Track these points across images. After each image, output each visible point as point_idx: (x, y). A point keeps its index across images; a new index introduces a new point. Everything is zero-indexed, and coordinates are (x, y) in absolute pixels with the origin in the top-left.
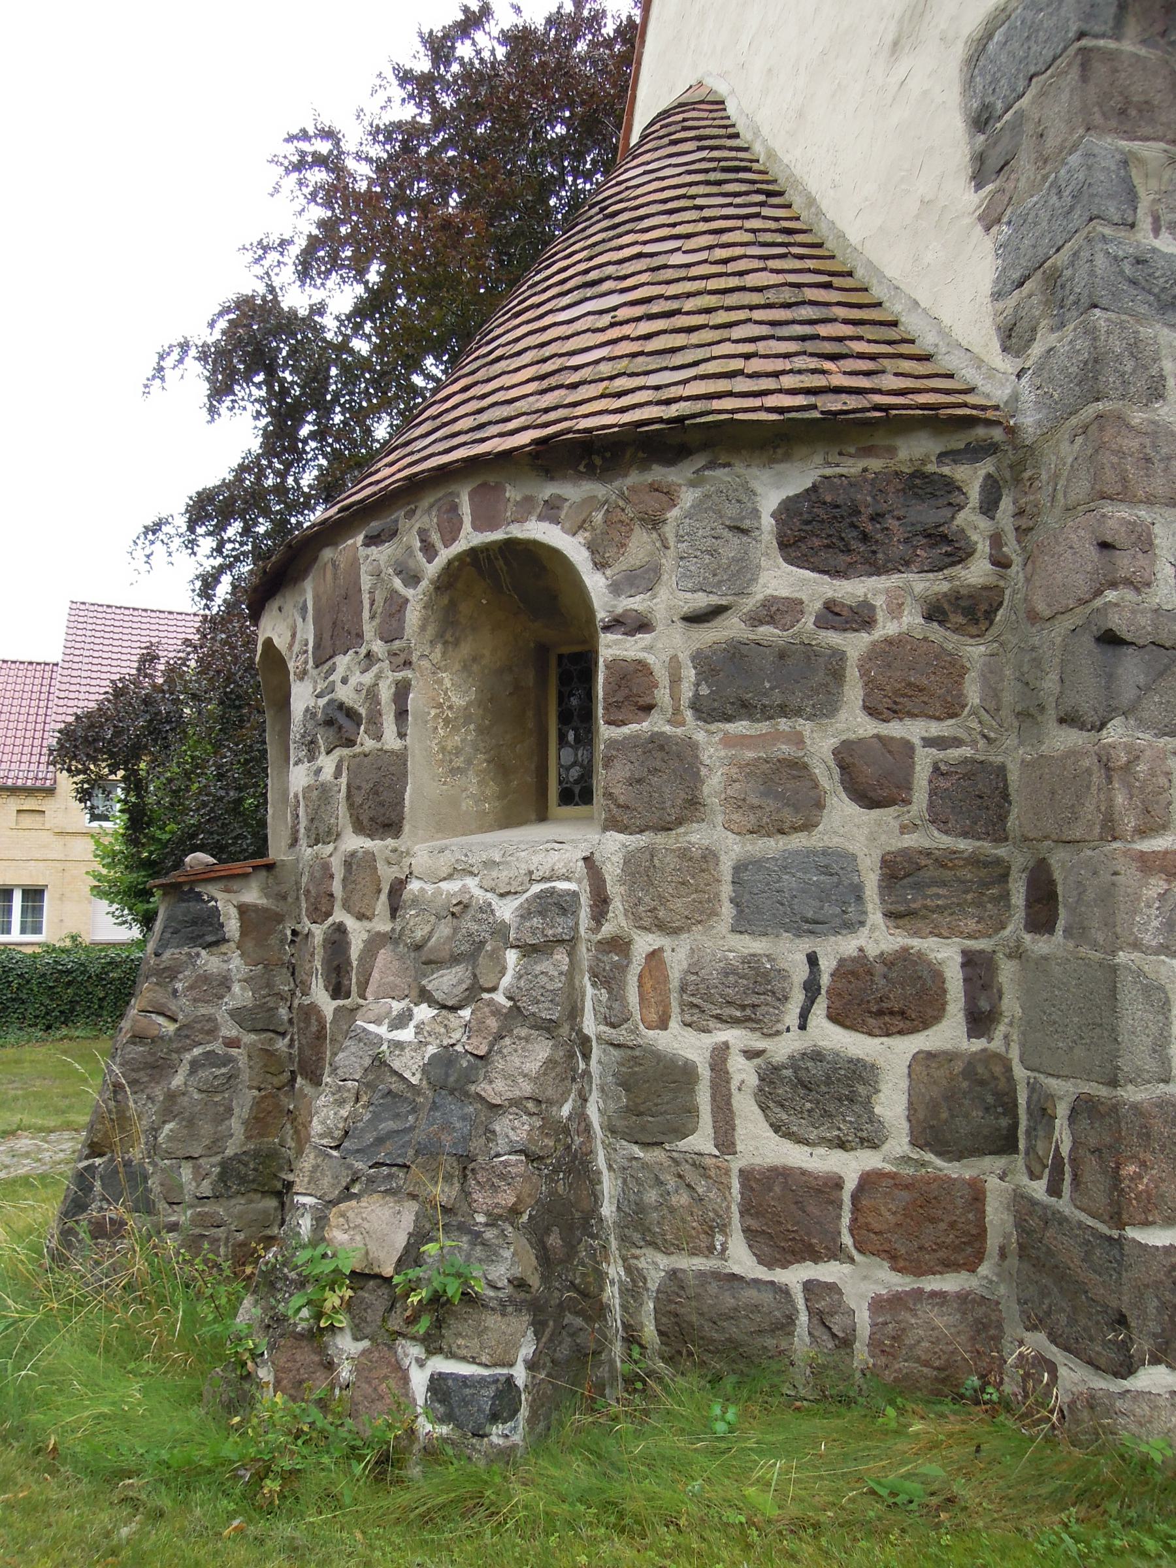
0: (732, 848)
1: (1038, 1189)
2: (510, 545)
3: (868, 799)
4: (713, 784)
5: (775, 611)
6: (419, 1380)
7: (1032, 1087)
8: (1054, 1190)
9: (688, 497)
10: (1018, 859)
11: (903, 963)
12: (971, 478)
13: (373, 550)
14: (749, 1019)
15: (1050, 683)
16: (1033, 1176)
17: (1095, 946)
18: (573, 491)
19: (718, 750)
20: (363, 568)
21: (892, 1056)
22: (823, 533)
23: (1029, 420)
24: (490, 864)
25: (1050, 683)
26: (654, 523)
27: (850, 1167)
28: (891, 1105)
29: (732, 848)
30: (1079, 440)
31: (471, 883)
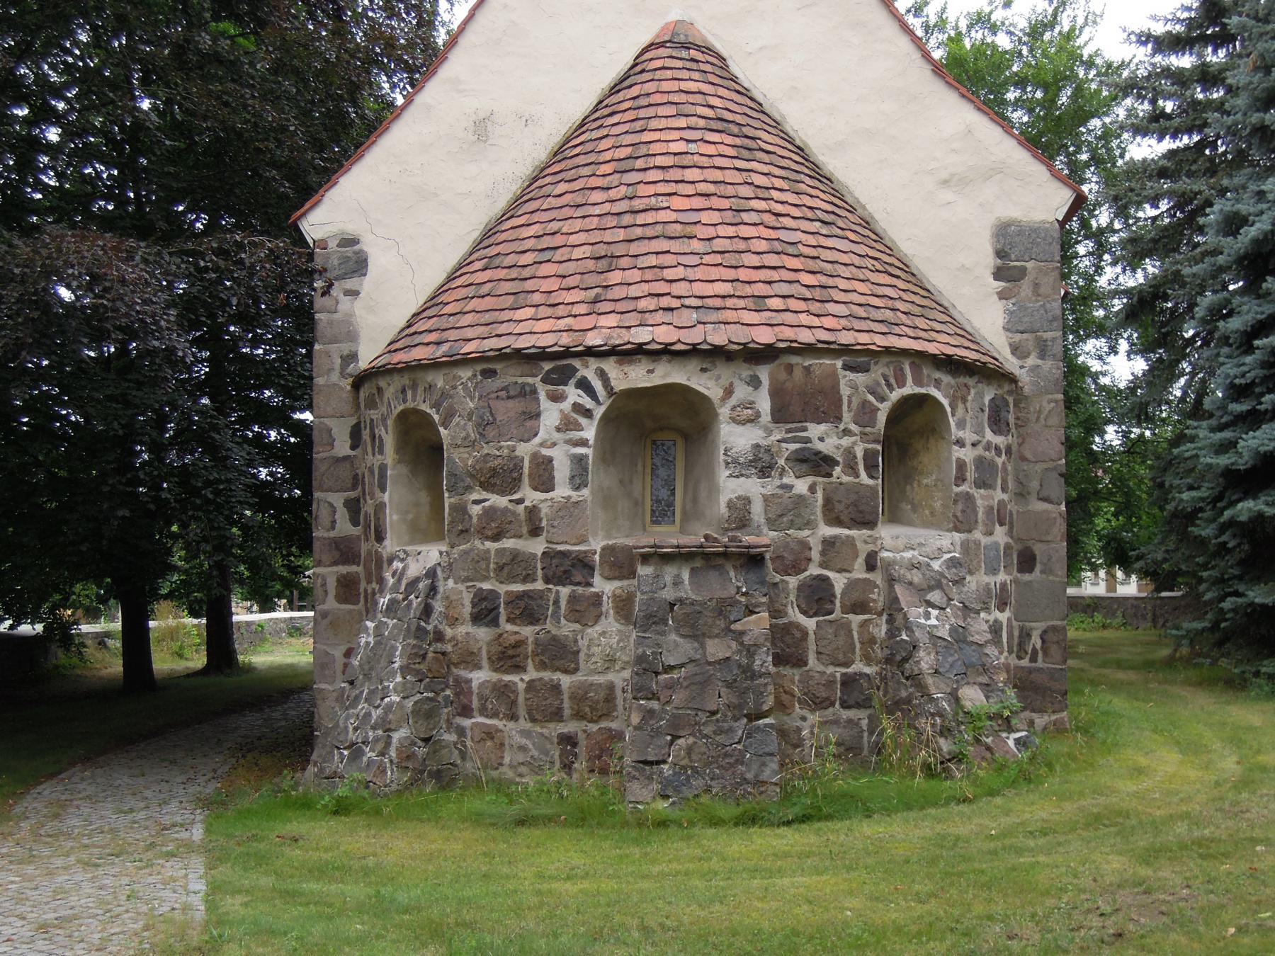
1: (1025, 663)
3: (1001, 524)
5: (988, 447)
8: (1034, 659)
12: (1011, 400)
13: (851, 375)
17: (1057, 576)
18: (946, 379)
19: (982, 499)
20: (842, 382)
21: (1003, 617)
24: (921, 545)
25: (1035, 485)
26: (964, 400)
30: (1053, 405)
31: (916, 553)
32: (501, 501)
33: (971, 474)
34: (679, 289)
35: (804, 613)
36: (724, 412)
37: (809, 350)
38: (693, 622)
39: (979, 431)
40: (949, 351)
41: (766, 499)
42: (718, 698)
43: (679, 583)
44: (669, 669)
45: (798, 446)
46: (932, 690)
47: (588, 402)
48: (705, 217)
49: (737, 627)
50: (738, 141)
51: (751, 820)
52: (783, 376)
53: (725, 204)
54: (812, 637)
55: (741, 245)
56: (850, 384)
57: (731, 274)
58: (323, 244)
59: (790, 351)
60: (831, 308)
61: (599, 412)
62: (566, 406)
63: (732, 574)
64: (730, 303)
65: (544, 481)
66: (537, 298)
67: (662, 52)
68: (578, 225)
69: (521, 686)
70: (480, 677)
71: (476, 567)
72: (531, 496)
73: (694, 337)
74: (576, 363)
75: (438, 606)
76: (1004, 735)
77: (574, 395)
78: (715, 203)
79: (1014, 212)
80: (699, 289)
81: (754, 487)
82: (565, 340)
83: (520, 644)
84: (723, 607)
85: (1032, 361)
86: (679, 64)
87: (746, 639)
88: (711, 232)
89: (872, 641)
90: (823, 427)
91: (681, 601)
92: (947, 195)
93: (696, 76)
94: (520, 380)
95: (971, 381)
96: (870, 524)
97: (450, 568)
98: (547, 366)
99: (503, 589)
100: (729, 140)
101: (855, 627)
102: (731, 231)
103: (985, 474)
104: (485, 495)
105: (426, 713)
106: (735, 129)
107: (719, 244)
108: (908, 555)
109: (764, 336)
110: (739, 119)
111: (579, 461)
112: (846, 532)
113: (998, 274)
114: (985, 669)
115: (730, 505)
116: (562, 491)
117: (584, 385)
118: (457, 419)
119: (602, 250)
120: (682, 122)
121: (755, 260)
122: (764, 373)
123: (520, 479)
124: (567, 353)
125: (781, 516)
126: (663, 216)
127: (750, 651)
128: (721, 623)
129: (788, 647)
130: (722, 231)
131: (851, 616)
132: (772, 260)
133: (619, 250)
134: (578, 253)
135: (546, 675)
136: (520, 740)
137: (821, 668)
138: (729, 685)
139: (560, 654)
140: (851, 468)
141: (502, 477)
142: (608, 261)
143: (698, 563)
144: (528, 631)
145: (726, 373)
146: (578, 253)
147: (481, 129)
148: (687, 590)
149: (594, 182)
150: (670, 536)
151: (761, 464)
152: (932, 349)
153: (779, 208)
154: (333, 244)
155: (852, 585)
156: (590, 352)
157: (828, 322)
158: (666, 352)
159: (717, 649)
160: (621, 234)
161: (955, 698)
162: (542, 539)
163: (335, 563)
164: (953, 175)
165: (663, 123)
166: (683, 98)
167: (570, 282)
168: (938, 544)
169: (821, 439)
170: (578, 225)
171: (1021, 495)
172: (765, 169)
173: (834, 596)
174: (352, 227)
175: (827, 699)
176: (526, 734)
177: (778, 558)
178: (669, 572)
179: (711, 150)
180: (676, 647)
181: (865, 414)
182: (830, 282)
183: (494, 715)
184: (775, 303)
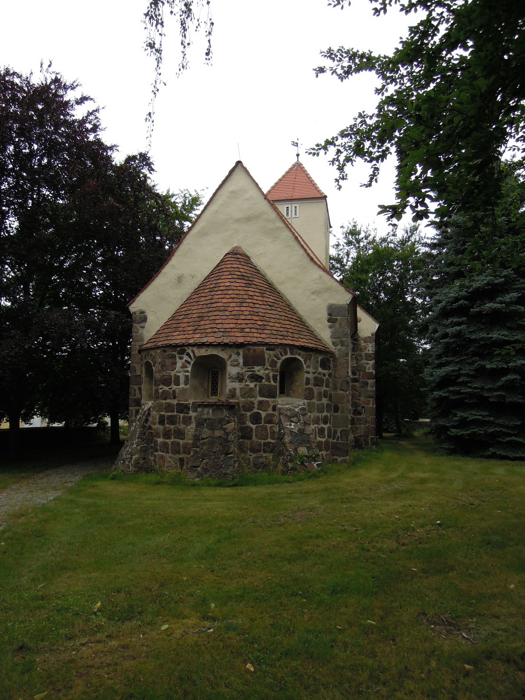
0: (317, 402)
1: (335, 441)
2: (295, 358)
4: (315, 395)
5: (320, 373)
6: (315, 465)
7: (334, 430)
8: (338, 440)
9: (313, 357)
10: (333, 405)
11: (327, 416)
12: (331, 359)
14: (318, 424)
15: (339, 385)
16: (334, 439)
18: (302, 353)
19: (316, 390)
20: (266, 354)
21: (326, 426)
22: (324, 365)
23: (337, 356)
24: (292, 403)
25: (339, 385)
26: (310, 359)
27: (323, 440)
28: (326, 433)
29: (317, 402)
32: (166, 388)
33: (312, 382)
34: (219, 326)
35: (252, 423)
36: (229, 363)
37: (255, 344)
38: (212, 425)
39: (316, 368)
40: (303, 344)
41: (241, 389)
42: (217, 448)
43: (208, 413)
44: (203, 439)
45: (251, 373)
46: (288, 448)
47: (189, 360)
48: (231, 305)
49: (224, 427)
50: (247, 282)
51: (220, 485)
52: (247, 352)
53: (239, 300)
54: (254, 430)
55: (241, 313)
56: (268, 354)
57: (235, 321)
58: (135, 313)
59: (248, 344)
60: (265, 331)
61: (192, 363)
62: (183, 360)
63: (225, 411)
64: (233, 330)
65: (177, 383)
66: (181, 329)
67: (229, 256)
68: (196, 307)
69: (170, 443)
70: (160, 440)
71: (160, 408)
72: (174, 387)
73: (219, 340)
74: (186, 348)
75: (150, 419)
76: (313, 463)
77: (186, 357)
78: (235, 300)
79: (334, 302)
80: (225, 326)
81: (237, 385)
82: (184, 341)
83: (170, 430)
84: (221, 421)
85: (339, 347)
86: (233, 259)
87: (227, 431)
88: (232, 309)
89: (274, 432)
90: (259, 367)
91: (209, 419)
92: (314, 297)
93: (238, 263)
94: (172, 353)
95: (312, 354)
96: (274, 397)
97: (154, 408)
98: (179, 349)
99: (166, 414)
100: (244, 282)
101: (268, 428)
102: (238, 309)
103: (318, 382)
104: (163, 386)
105: (144, 450)
106: (246, 278)
107: (234, 313)
108: (287, 406)
109: (241, 340)
110: (249, 275)
111: (187, 377)
112: (266, 399)
113: (329, 321)
114: (309, 442)
115: (230, 390)
116: (182, 386)
117: (188, 354)
118: (157, 364)
119: (201, 315)
120: (230, 277)
121: (244, 317)
122: (241, 351)
123: (171, 382)
124: (183, 345)
125: (245, 394)
126: (219, 304)
127: (227, 434)
128: (220, 426)
129: (246, 433)
130: (236, 309)
131: (267, 425)
132: (249, 317)
133: (205, 315)
134: (194, 316)
135: (176, 440)
136: (169, 459)
137: (257, 440)
138: (220, 444)
139: (180, 434)
140: (268, 379)
141: (167, 382)
142: (201, 318)
143: (215, 407)
144: (172, 427)
145: (229, 351)
146: (194, 316)
147: (180, 279)
148: (211, 416)
149: (203, 295)
150: (213, 399)
151: (240, 378)
152: (297, 344)
153: (255, 302)
154: (138, 313)
155: (268, 415)
156: (190, 345)
157: (263, 336)
158: (210, 345)
159: (218, 433)
160: (207, 310)
161: (296, 450)
162: (176, 400)
163: (135, 406)
164: (315, 291)
165: (225, 277)
166: (232, 269)
167: (190, 324)
168: (298, 403)
169: (259, 371)
170: (196, 307)
171: (335, 388)
172: (253, 290)
173: (261, 418)
174: (143, 308)
175: (258, 450)
176: (171, 457)
177: (244, 407)
178: (206, 410)
179: (237, 285)
180: (206, 432)
181: (273, 364)
182: (267, 323)
183: (163, 452)
184: (247, 330)
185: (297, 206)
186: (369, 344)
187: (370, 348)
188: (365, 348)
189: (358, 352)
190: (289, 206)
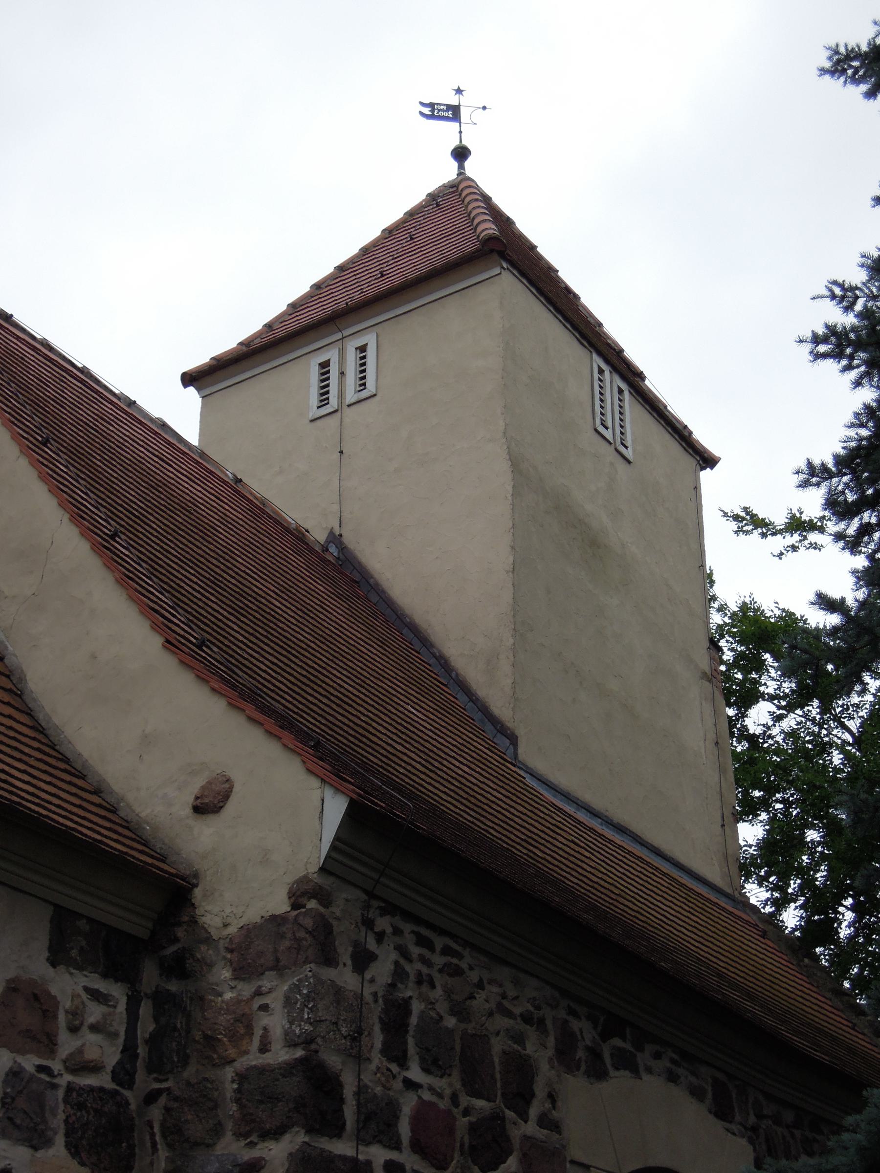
185: (369, 339)
186: (266, 983)
187: (275, 1022)
188: (243, 1023)
189: (190, 1073)
190: (332, 355)
